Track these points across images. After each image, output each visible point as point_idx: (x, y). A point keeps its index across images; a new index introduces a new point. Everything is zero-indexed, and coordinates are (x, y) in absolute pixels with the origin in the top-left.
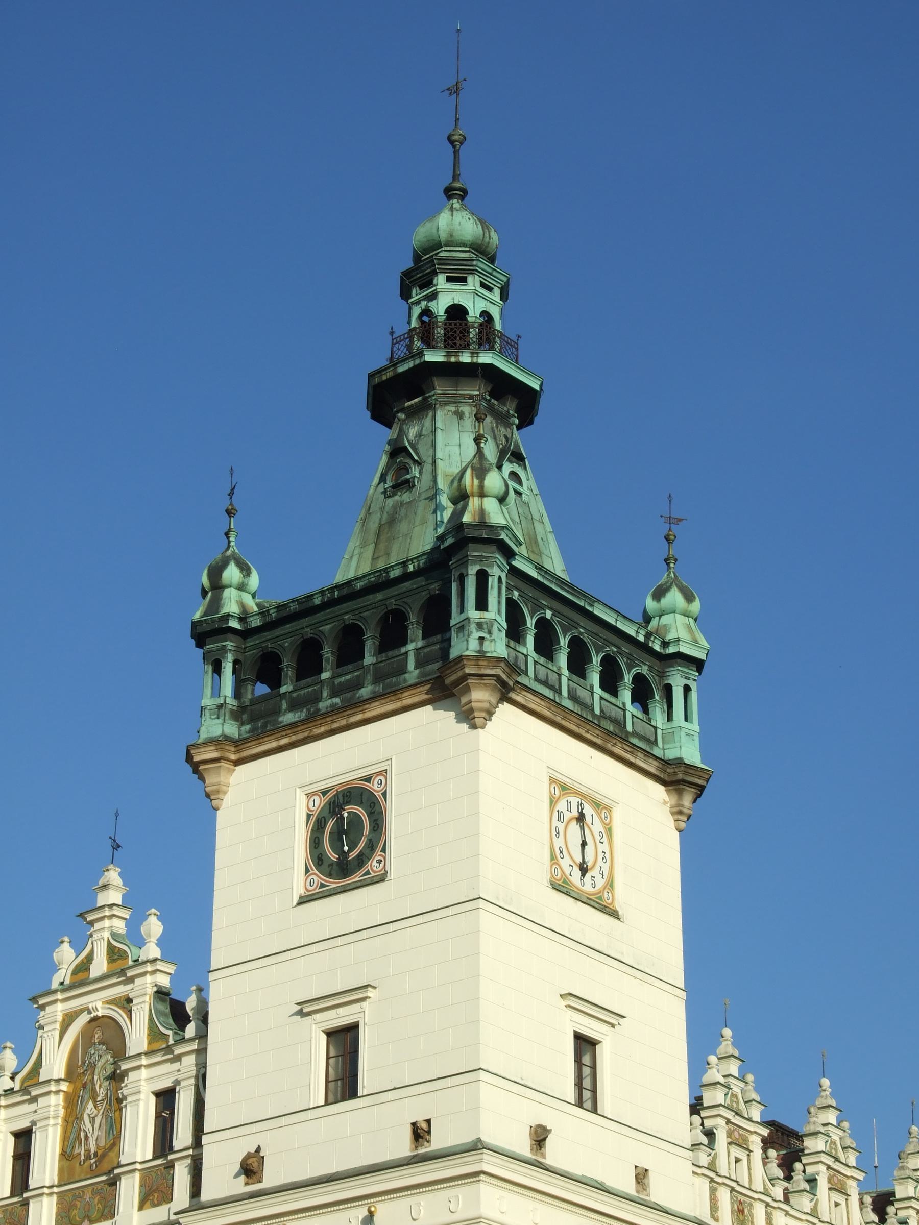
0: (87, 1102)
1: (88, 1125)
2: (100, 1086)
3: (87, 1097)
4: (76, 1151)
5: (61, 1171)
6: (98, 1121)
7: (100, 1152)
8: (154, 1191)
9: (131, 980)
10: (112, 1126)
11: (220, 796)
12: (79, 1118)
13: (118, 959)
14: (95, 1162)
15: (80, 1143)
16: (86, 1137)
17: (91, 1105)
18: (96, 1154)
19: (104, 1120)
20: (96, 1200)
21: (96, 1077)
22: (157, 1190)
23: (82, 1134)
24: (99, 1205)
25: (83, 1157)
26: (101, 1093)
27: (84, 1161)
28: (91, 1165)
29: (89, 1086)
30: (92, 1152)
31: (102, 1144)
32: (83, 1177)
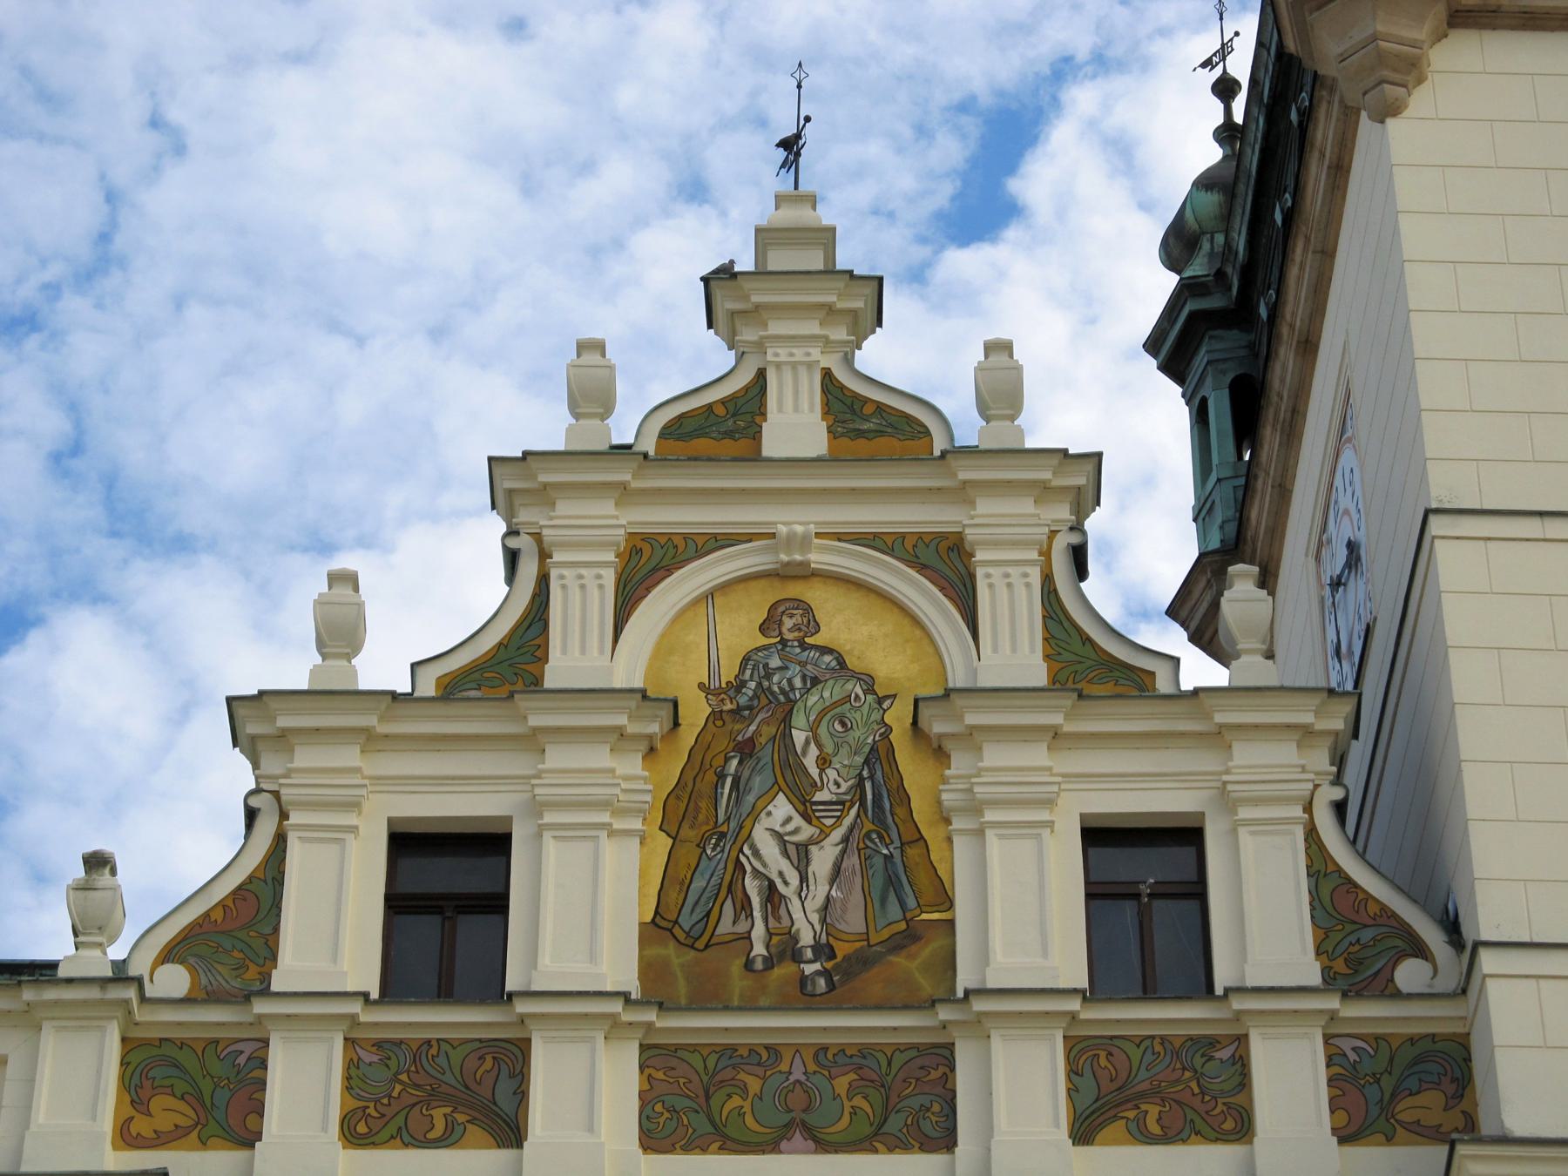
0: (768, 796)
1: (775, 860)
2: (824, 762)
3: (758, 783)
4: (726, 926)
5: (650, 970)
6: (822, 860)
7: (842, 949)
8: (1143, 1096)
9: (964, 493)
10: (892, 882)
11: (1410, 79)
12: (731, 836)
13: (879, 433)
14: (825, 973)
15: (745, 906)
16: (772, 895)
17: (781, 808)
18: (823, 950)
19: (853, 861)
20: (842, 1084)
21: (799, 737)
22: (1154, 1093)
23: (752, 886)
24: (858, 1101)
25: (759, 949)
26: (832, 785)
27: (769, 963)
28: (803, 980)
29: (765, 755)
30: (806, 939)
31: (853, 921)
32: (763, 1002)
